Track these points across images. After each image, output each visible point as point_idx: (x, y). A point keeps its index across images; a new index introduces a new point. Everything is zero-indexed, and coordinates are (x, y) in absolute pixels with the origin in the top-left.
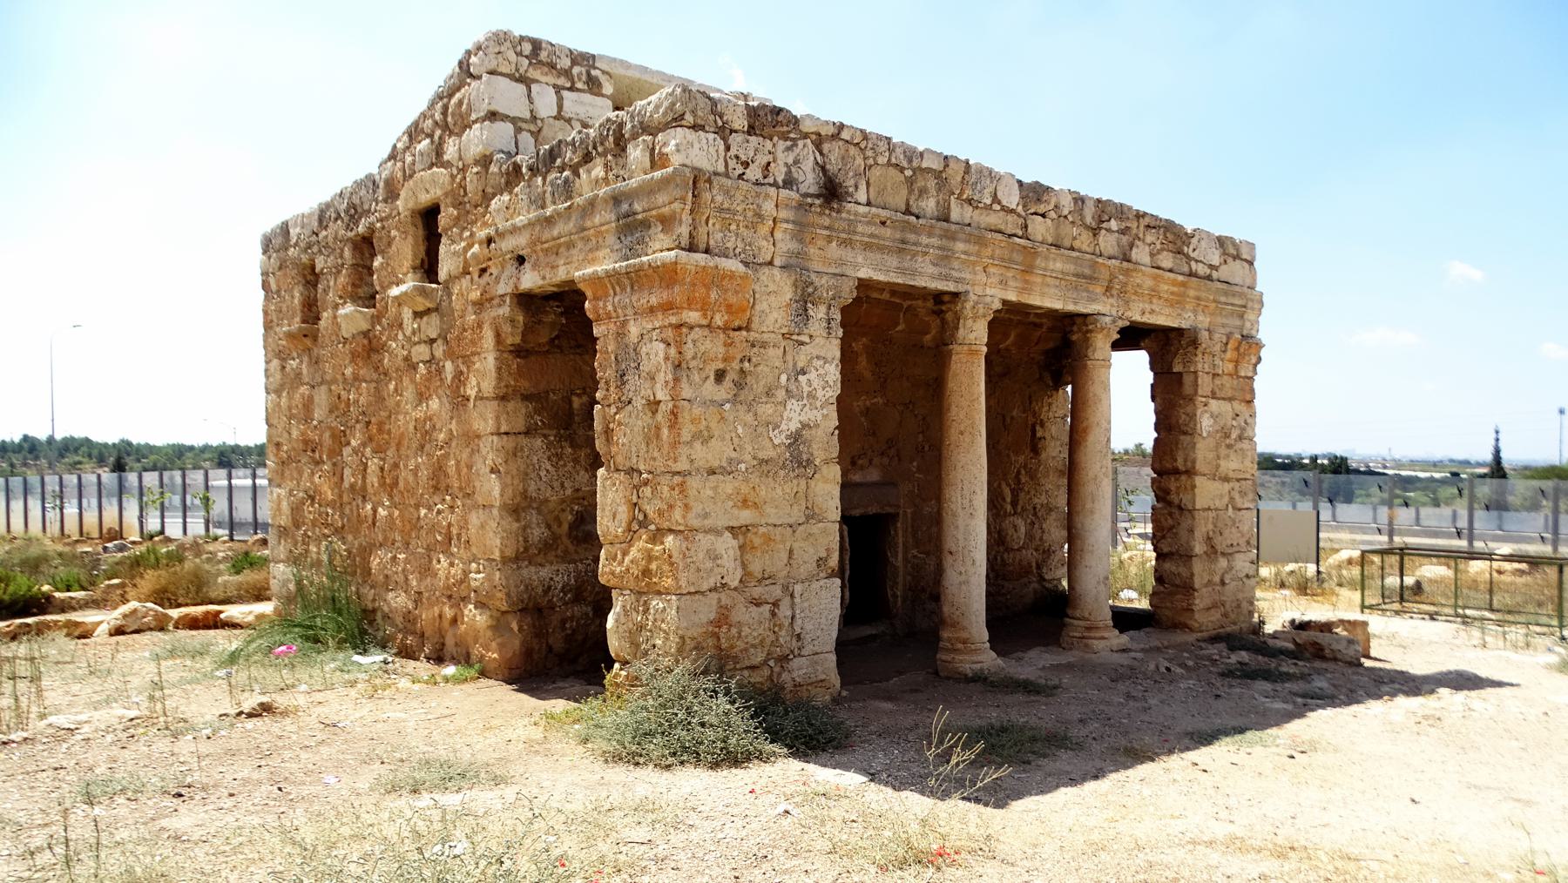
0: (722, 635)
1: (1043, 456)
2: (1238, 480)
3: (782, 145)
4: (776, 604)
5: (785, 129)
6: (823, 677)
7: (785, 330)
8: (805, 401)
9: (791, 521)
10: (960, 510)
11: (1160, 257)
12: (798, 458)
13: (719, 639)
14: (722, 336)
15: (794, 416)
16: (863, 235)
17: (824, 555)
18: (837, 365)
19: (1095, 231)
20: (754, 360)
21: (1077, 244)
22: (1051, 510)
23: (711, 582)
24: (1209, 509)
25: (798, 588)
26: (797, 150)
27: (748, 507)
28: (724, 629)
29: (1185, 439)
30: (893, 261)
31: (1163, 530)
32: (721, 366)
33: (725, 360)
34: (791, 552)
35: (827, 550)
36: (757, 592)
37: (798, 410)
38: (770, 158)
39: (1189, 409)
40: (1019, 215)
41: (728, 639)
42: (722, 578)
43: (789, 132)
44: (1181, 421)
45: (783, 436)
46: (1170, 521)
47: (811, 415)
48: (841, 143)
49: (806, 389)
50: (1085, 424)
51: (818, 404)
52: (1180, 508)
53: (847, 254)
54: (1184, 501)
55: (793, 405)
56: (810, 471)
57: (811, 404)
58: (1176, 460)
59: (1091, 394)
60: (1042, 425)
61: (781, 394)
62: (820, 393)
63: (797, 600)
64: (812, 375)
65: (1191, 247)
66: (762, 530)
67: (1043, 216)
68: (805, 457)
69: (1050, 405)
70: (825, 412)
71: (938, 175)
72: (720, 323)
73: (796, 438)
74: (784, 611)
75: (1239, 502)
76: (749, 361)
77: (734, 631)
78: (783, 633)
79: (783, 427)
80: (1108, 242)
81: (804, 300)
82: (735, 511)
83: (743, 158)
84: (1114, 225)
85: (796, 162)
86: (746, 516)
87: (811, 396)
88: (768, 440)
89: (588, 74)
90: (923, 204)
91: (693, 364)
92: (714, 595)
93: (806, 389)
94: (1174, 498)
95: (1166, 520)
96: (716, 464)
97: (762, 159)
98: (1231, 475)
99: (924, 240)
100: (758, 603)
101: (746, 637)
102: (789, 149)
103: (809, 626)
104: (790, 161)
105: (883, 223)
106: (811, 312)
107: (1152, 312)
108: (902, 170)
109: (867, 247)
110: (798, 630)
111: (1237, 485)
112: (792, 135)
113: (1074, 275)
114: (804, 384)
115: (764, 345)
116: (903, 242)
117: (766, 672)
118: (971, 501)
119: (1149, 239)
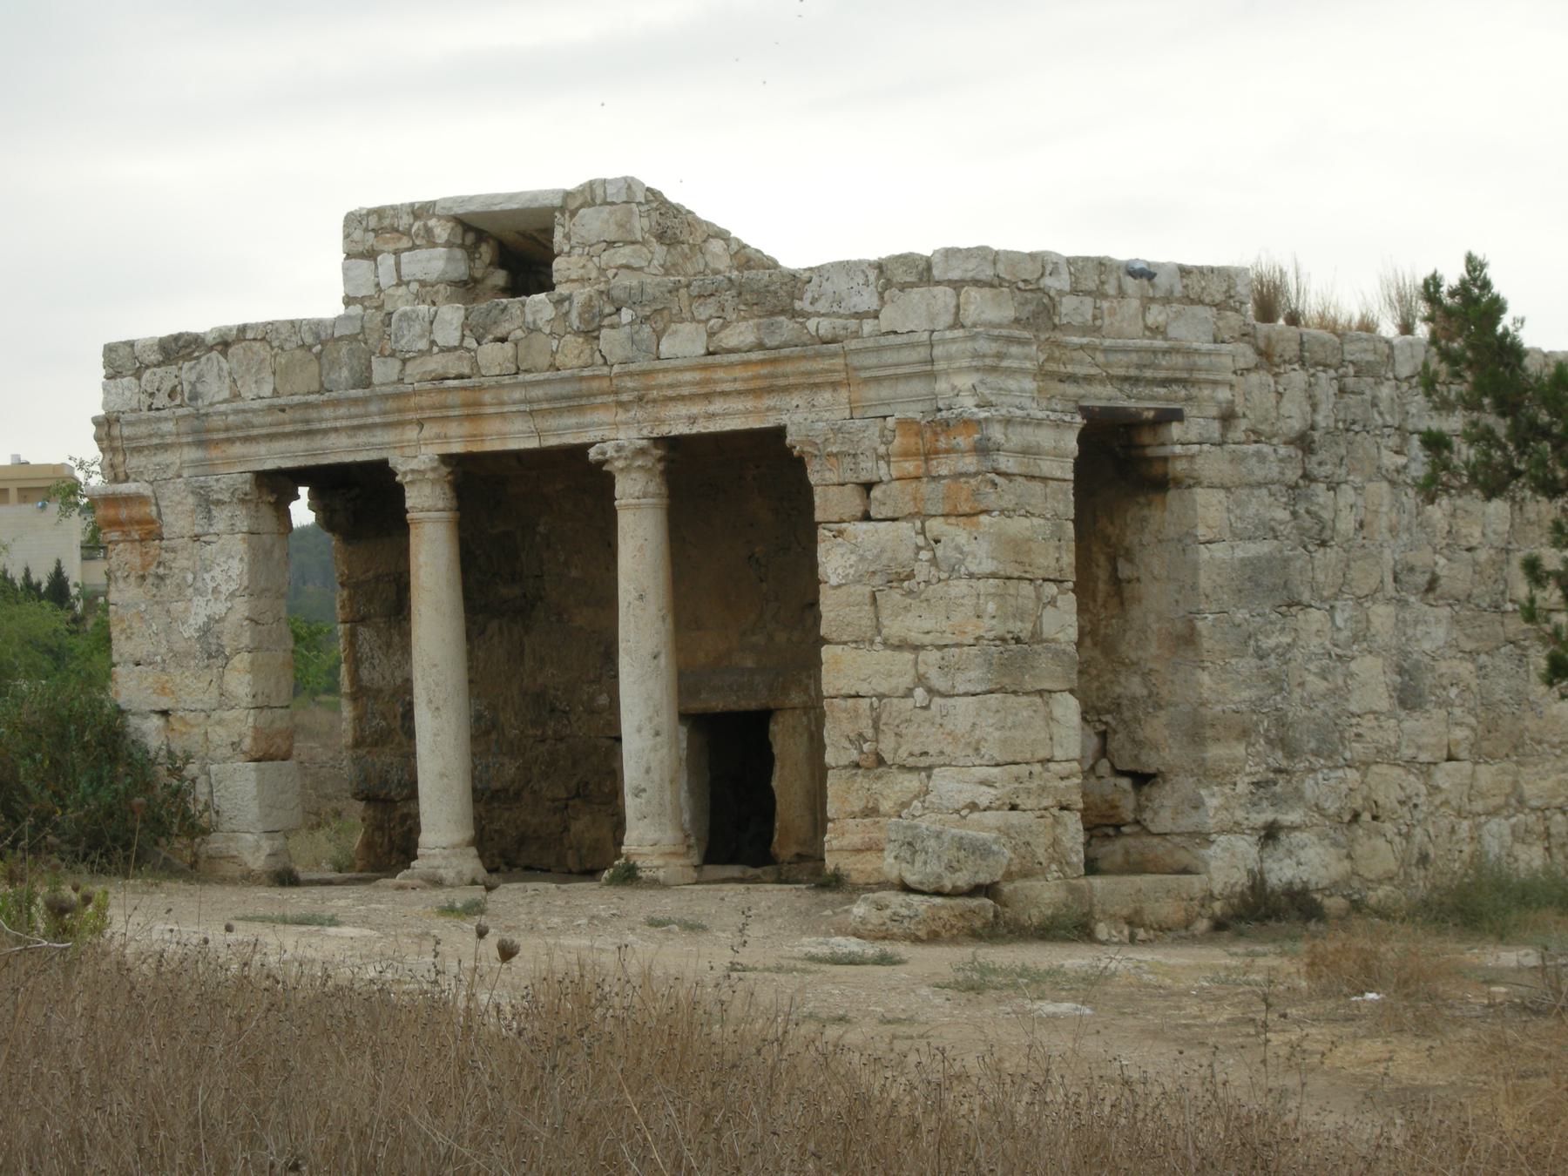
1: (1135, 612)
2: (940, 647)
3: (187, 365)
5: (188, 350)
6: (235, 853)
7: (191, 533)
8: (210, 597)
11: (722, 335)
12: (212, 651)
14: (137, 544)
15: (200, 611)
16: (262, 426)
17: (236, 739)
18: (241, 559)
19: (590, 334)
21: (559, 360)
22: (1158, 706)
24: (858, 696)
25: (214, 768)
26: (199, 367)
27: (165, 694)
30: (299, 445)
32: (141, 573)
33: (144, 567)
34: (206, 733)
35: (239, 735)
37: (204, 604)
38: (176, 381)
40: (468, 350)
43: (193, 352)
47: (219, 608)
48: (244, 344)
51: (223, 597)
53: (251, 449)
55: (199, 601)
56: (220, 661)
57: (216, 599)
60: (1129, 556)
62: (223, 588)
64: (217, 572)
65: (808, 296)
66: (180, 713)
67: (503, 340)
68: (214, 648)
69: (1144, 519)
70: (229, 605)
71: (352, 338)
72: (137, 537)
73: (205, 631)
75: (939, 683)
79: (191, 621)
80: (612, 341)
81: (206, 502)
82: (154, 697)
83: (150, 390)
84: (626, 315)
85: (200, 378)
86: (165, 704)
87: (215, 590)
89: (425, 225)
90: (334, 376)
91: (119, 574)
93: (211, 585)
96: (138, 656)
97: (167, 386)
98: (915, 637)
99: (328, 412)
102: (191, 368)
104: (193, 378)
105: (283, 411)
107: (711, 416)
108: (310, 348)
109: (271, 437)
111: (932, 656)
112: (196, 354)
113: (548, 400)
114: (208, 581)
115: (174, 550)
116: (307, 422)
119: (703, 312)
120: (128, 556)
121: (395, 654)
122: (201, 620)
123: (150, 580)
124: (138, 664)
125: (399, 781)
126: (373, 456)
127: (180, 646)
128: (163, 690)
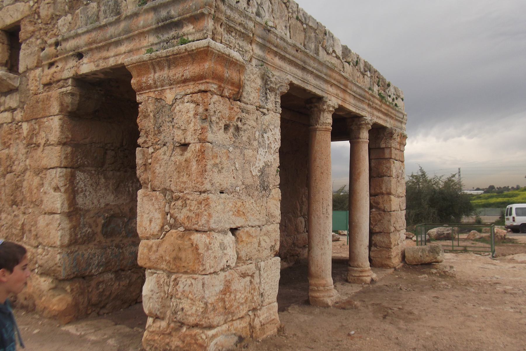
0: (226, 299)
4: (252, 276)
9: (260, 224)
10: (322, 215)
13: (225, 302)
20: (243, 121)
23: (221, 266)
25: (262, 264)
28: (228, 296)
29: (385, 178)
31: (376, 222)
36: (243, 268)
39: (388, 165)
41: (230, 302)
42: (227, 261)
44: (384, 171)
45: (257, 171)
46: (379, 217)
49: (267, 142)
50: (359, 171)
52: (384, 211)
54: (386, 208)
58: (382, 189)
59: (361, 156)
61: (255, 143)
62: (273, 146)
63: (262, 272)
66: (246, 229)
74: (257, 280)
76: (241, 121)
77: (232, 296)
78: (256, 294)
79: (257, 165)
82: (233, 218)
86: (238, 222)
87: (269, 147)
88: (249, 173)
92: (222, 274)
94: (381, 206)
95: (378, 216)
96: (225, 186)
100: (244, 275)
101: (239, 298)
103: (267, 288)
106: (269, 97)
110: (262, 291)
114: (266, 138)
116: (305, 62)
117: (247, 319)
118: (327, 210)
120: (221, 108)
121: (100, 189)
122: (262, 164)
123: (232, 130)
124: (222, 192)
125: (99, 263)
126: (319, 92)
127: (249, 181)
128: (238, 213)
